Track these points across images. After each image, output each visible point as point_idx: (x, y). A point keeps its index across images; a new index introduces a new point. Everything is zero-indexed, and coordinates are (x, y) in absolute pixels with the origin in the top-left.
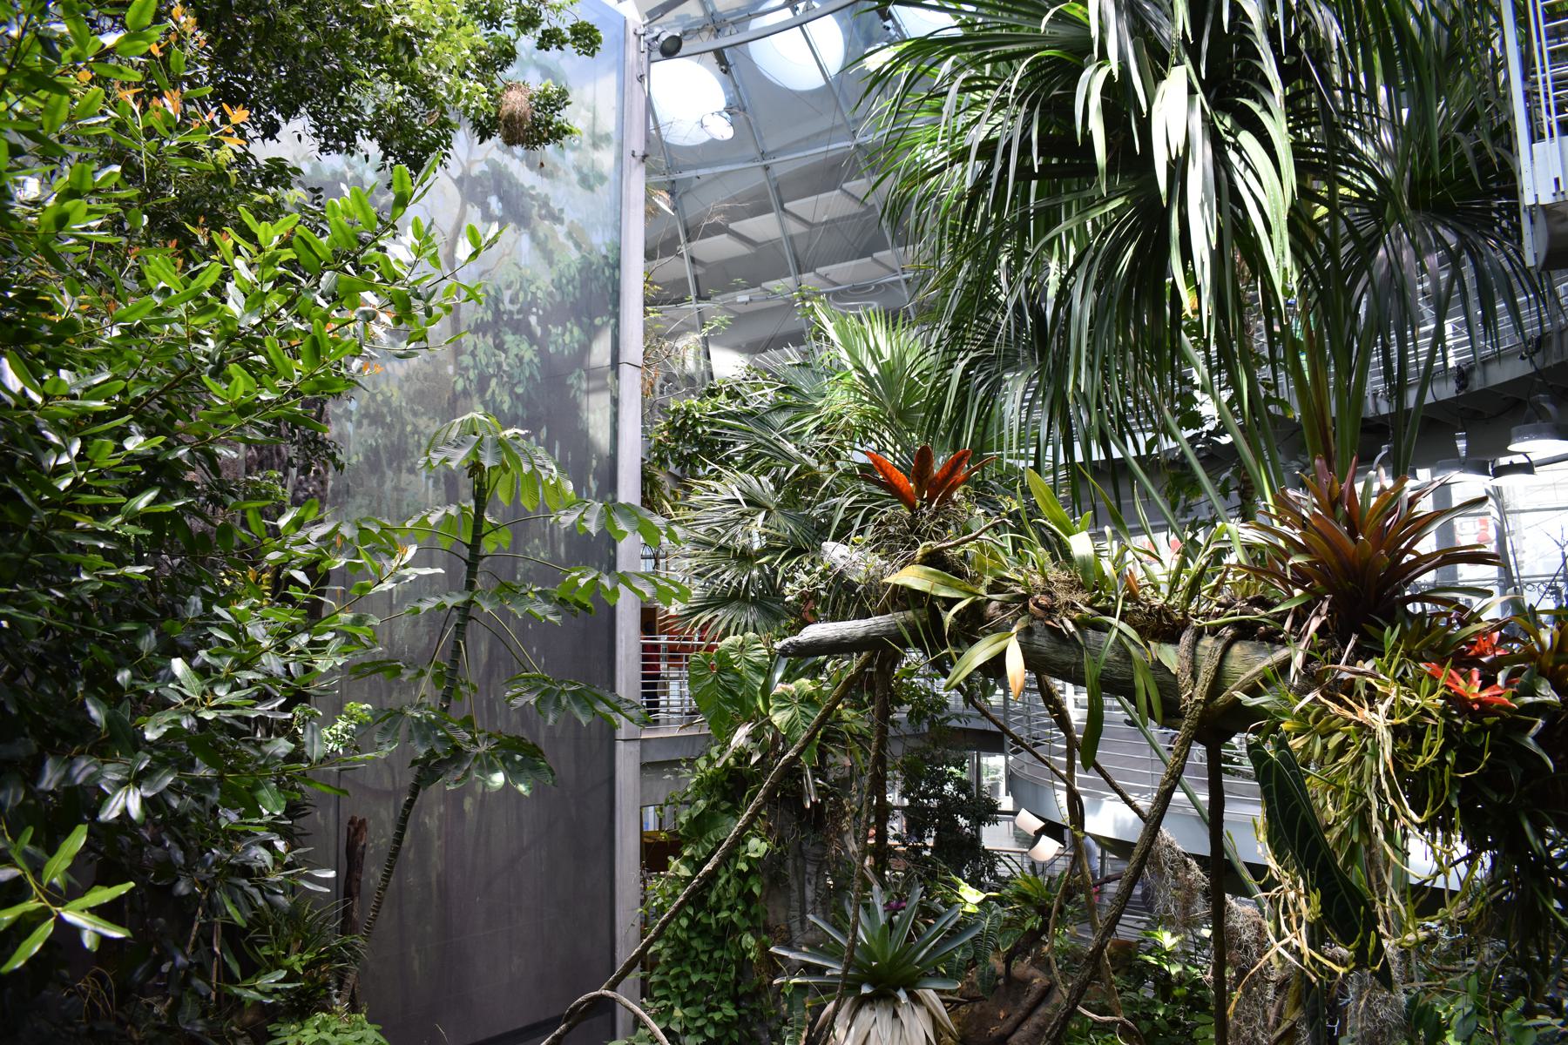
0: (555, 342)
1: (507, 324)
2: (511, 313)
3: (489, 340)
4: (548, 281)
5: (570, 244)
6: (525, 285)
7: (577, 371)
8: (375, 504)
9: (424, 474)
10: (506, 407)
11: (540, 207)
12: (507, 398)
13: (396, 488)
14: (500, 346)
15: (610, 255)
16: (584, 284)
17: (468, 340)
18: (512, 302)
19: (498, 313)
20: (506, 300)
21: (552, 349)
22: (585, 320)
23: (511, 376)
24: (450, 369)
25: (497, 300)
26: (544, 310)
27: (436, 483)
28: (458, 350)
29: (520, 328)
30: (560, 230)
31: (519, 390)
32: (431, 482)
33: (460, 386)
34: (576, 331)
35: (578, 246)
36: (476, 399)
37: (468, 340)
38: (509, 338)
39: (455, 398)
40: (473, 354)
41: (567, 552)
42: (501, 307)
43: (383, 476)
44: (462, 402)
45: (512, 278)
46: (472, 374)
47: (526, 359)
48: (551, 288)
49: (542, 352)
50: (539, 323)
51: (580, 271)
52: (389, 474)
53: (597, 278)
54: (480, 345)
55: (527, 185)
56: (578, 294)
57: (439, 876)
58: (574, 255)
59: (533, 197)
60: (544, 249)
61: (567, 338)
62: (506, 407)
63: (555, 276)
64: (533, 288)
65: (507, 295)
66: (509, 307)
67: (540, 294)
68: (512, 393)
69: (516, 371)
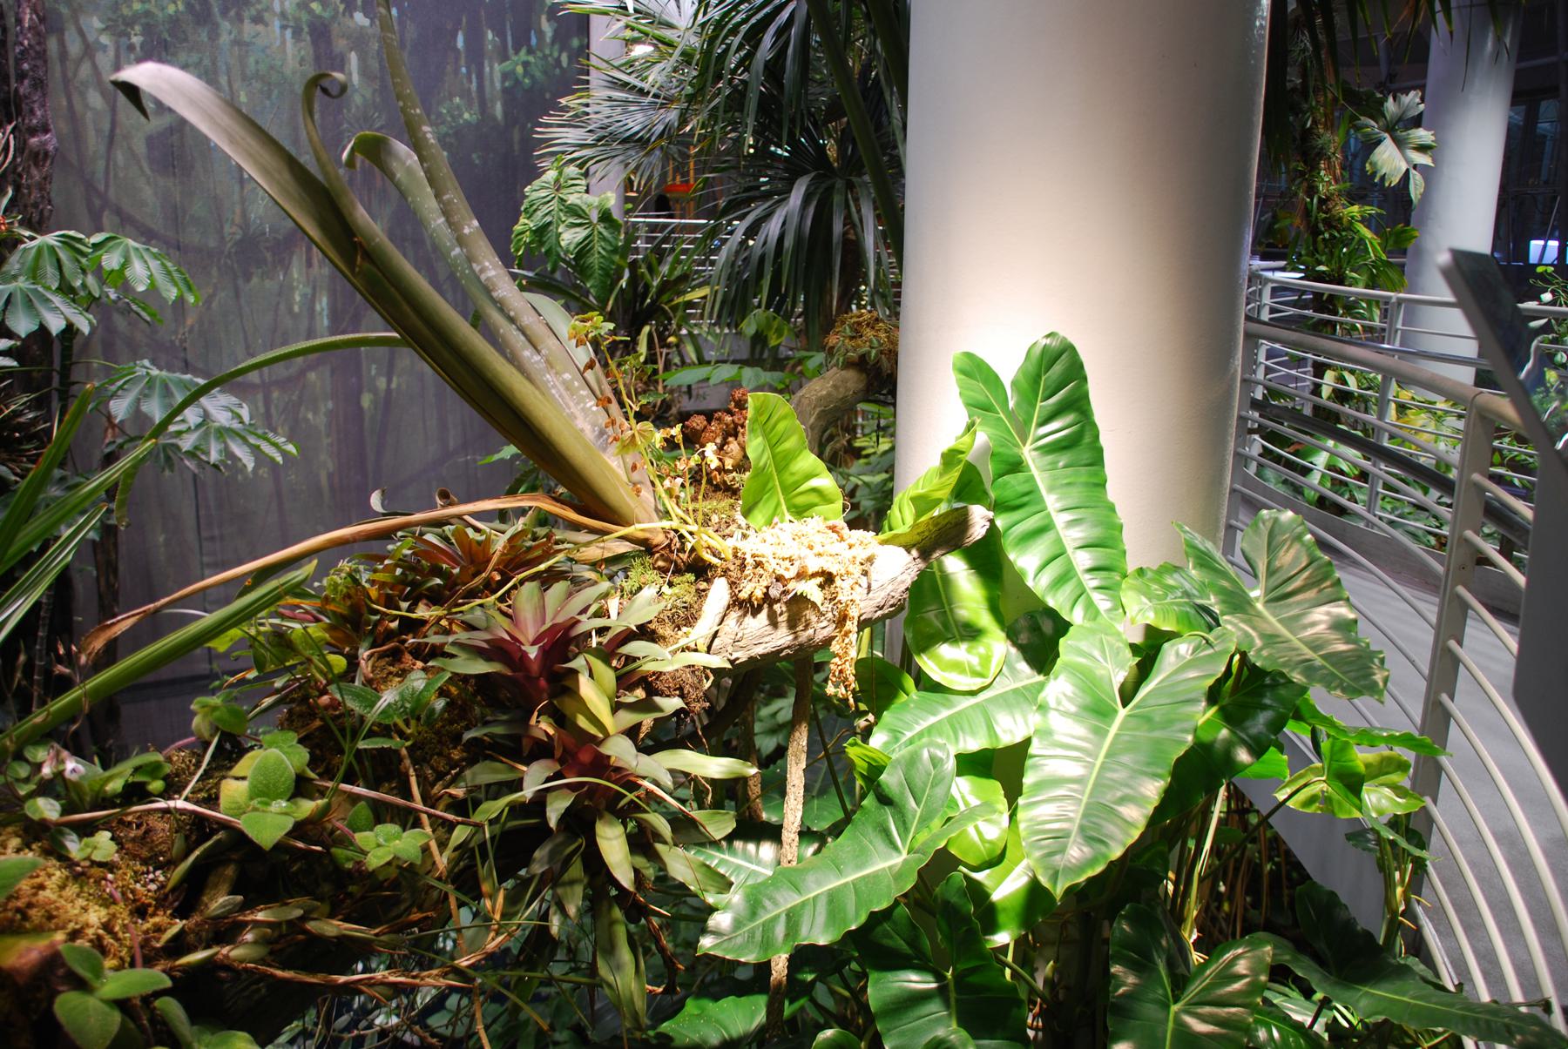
8: (207, 62)
9: (277, 23)
13: (238, 42)
27: (297, 33)
32: (288, 33)
41: (505, 113)
43: (216, 26)
52: (225, 25)
57: (330, 476)
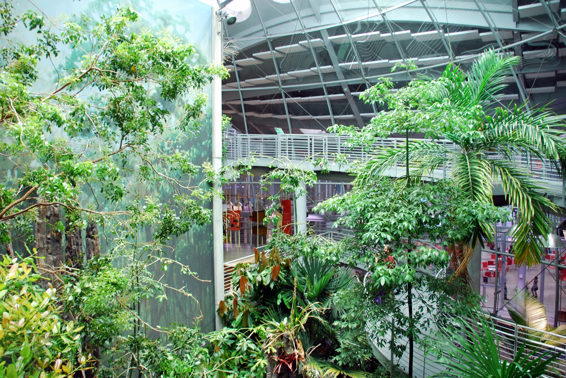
6: (174, 137)
10: (168, 191)
11: (179, 102)
12: (168, 187)
15: (208, 114)
18: (168, 146)
22: (198, 144)
26: (182, 145)
33: (149, 188)
34: (195, 150)
41: (194, 241)
45: (168, 136)
62: (168, 191)
64: (177, 138)
65: (166, 144)
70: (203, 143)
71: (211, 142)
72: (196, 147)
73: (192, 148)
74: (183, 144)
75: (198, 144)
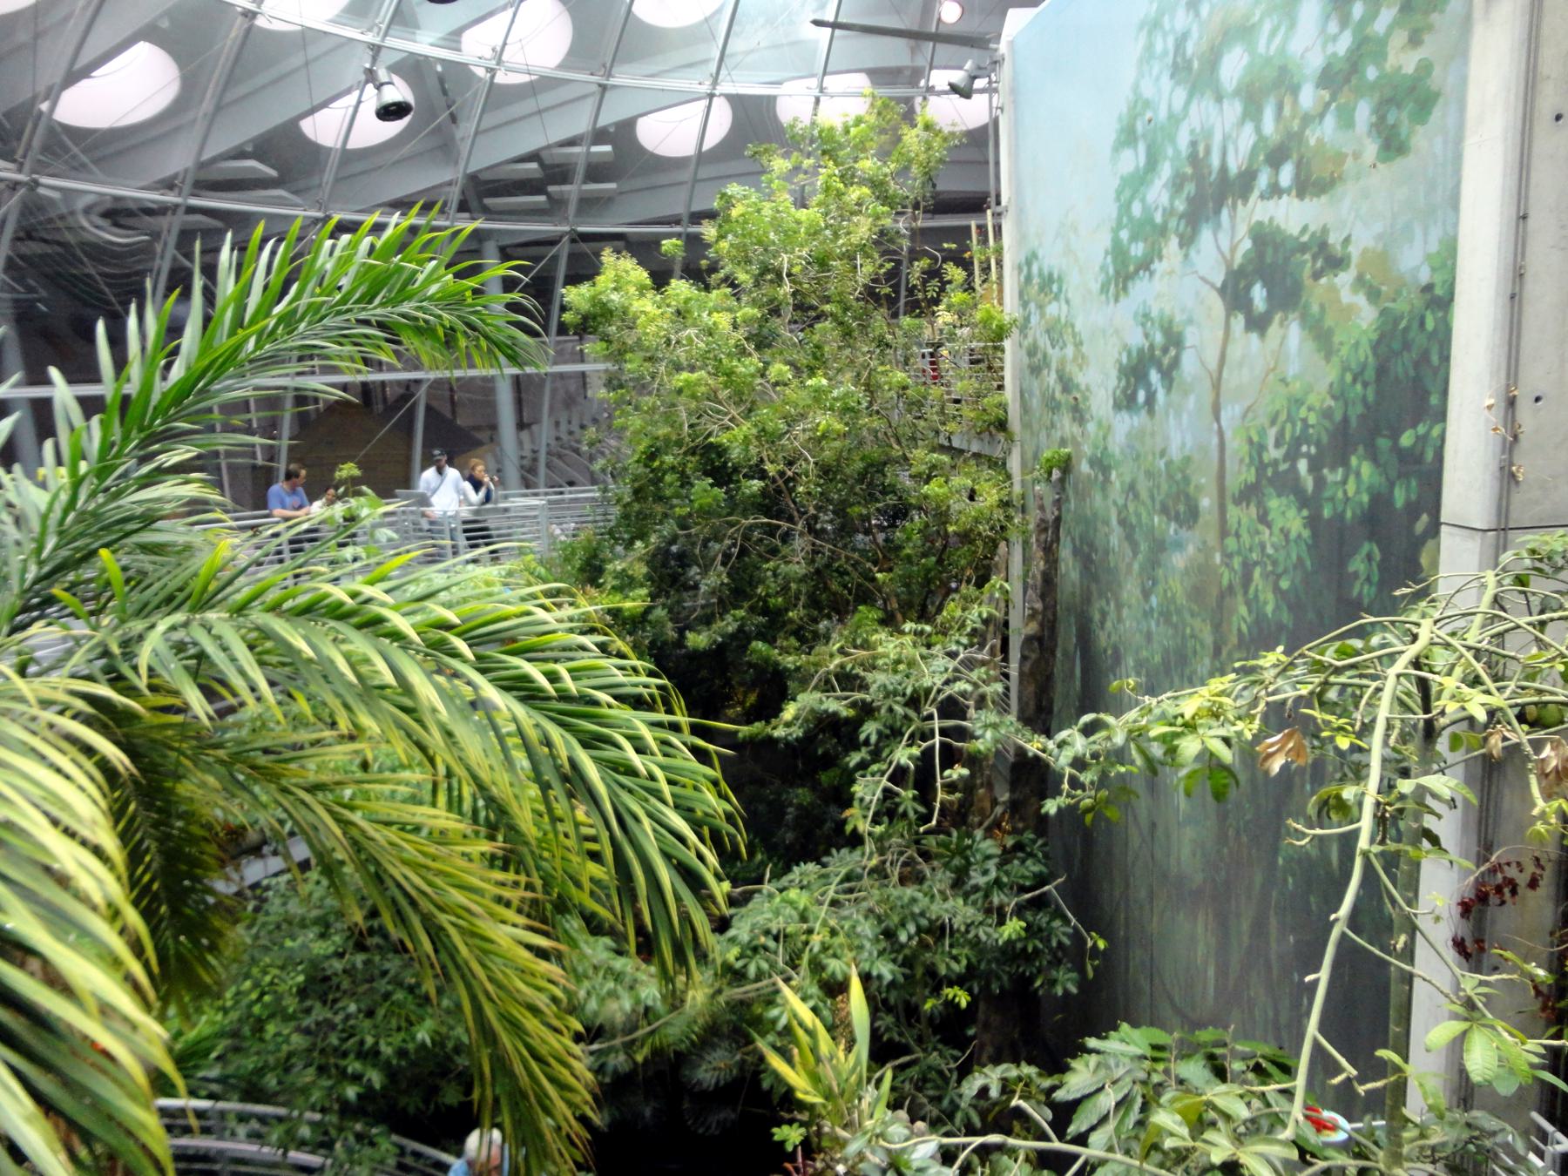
0: (1332, 499)
1: (1271, 481)
2: (1275, 463)
3: (1253, 510)
4: (1322, 387)
5: (1361, 300)
7: (1366, 547)
11: (1315, 258)
12: (1270, 597)
14: (1263, 519)
15: (1438, 279)
16: (1382, 371)
17: (1233, 512)
18: (1278, 445)
19: (1261, 467)
20: (1271, 442)
21: (1327, 512)
23: (1275, 563)
24: (1218, 558)
25: (1261, 448)
26: (1318, 444)
28: (1224, 533)
29: (1287, 484)
30: (1345, 279)
31: (1285, 584)
34: (1366, 469)
35: (1373, 295)
36: (1240, 598)
37: (1233, 512)
38: (1274, 503)
39: (1222, 596)
40: (1238, 535)
42: (1266, 458)
44: (1228, 600)
45: (1278, 407)
46: (1237, 562)
47: (1293, 535)
48: (1330, 402)
49: (1313, 522)
50: (1311, 469)
51: (1375, 347)
53: (1407, 346)
54: (1244, 521)
55: (1295, 231)
56: (1371, 397)
58: (1366, 316)
59: (1303, 248)
60: (1322, 336)
61: (1351, 487)
62: (1269, 609)
63: (1331, 374)
64: (1303, 412)
66: (1273, 453)
67: (1312, 419)
68: (1277, 589)
69: (1281, 556)
70: (1406, 440)
71: (1442, 438)
72: (1373, 456)
73: (1354, 461)
74: (1325, 439)
75: (1383, 443)
